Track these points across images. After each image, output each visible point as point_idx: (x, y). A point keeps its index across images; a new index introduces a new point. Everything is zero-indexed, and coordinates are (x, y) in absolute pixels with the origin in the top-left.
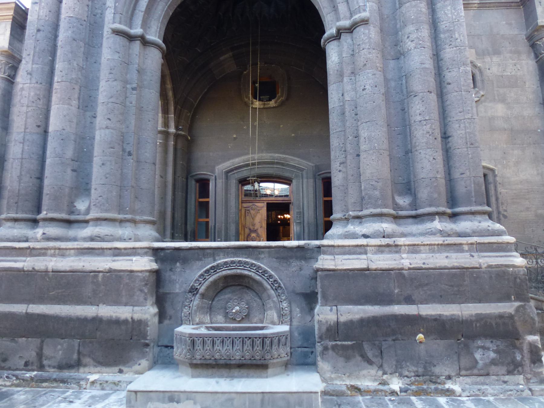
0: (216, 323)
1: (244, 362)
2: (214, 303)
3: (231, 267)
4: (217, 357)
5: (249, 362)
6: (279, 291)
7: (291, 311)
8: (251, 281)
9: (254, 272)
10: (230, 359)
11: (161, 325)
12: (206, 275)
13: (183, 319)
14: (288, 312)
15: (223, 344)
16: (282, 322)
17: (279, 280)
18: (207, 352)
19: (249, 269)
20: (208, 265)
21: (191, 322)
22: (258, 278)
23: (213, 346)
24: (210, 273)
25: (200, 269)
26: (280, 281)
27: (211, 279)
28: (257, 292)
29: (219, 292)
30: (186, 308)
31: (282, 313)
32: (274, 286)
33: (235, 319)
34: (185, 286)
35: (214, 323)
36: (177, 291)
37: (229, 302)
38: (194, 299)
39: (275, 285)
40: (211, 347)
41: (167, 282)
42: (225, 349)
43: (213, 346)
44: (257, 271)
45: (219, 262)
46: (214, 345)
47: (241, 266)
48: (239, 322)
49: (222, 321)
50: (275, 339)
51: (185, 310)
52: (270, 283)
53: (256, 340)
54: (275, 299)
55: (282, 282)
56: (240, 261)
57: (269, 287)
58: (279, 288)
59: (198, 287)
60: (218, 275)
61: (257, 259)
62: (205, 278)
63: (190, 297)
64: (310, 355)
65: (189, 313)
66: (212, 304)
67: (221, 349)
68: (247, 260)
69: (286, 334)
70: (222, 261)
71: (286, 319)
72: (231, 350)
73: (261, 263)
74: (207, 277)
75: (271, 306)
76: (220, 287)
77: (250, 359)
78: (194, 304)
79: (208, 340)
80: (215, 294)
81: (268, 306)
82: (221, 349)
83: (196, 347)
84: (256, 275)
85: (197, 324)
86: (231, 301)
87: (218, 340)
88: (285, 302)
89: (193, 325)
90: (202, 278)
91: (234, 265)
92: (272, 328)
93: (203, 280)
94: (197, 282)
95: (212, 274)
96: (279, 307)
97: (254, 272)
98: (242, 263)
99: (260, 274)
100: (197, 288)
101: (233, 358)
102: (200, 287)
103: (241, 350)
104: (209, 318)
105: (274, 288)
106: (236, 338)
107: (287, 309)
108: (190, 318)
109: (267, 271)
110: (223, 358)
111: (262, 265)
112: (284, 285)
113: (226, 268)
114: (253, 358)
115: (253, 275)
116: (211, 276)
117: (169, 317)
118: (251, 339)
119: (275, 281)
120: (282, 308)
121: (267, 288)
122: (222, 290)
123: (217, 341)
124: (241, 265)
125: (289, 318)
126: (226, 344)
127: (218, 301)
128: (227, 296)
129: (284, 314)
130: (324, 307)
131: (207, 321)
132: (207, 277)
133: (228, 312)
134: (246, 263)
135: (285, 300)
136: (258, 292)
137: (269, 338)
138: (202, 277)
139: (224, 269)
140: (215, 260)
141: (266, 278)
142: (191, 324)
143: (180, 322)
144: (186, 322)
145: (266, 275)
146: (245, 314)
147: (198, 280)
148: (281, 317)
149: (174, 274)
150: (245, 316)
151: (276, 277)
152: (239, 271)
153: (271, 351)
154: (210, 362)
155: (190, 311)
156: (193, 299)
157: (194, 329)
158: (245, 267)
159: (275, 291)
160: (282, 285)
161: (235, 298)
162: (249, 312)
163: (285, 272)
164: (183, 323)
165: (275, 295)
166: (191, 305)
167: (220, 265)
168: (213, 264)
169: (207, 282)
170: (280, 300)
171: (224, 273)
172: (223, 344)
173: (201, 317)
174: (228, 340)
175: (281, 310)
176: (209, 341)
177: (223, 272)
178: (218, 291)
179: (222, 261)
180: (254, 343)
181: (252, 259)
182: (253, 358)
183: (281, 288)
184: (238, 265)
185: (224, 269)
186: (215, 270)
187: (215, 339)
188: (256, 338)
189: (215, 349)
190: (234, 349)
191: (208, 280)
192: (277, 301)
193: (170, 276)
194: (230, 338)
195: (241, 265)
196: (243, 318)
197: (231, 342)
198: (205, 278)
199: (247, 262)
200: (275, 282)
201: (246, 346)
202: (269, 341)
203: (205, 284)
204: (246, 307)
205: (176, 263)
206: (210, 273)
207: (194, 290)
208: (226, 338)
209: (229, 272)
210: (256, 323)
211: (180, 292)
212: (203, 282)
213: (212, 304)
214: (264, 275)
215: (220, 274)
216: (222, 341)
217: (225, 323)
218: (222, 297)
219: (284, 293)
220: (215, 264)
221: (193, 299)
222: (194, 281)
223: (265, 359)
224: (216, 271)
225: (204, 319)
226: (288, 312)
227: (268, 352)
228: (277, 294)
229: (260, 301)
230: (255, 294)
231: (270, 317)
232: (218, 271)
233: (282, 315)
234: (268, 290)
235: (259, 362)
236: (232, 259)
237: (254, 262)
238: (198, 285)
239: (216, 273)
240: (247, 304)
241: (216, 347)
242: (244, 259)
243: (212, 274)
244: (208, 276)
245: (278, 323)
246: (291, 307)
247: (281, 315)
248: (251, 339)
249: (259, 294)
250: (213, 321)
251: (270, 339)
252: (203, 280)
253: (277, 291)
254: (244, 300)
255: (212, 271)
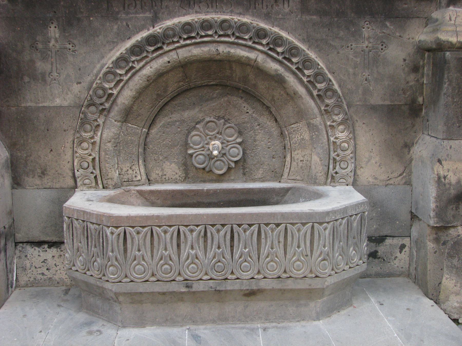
0: (162, 182)
1: (263, 284)
2: (154, 131)
3: (202, 37)
4: (188, 274)
5: (276, 285)
6: (327, 101)
7: (355, 152)
8: (251, 77)
9: (262, 52)
10: (226, 279)
11: (18, 192)
12: (133, 58)
13: (77, 174)
14: (349, 152)
15: (205, 241)
16: (333, 177)
17: (327, 72)
18: (162, 262)
19: (250, 43)
20: (138, 33)
21: (100, 182)
22: (273, 66)
23: (179, 246)
24: (145, 54)
25: (114, 44)
26: (330, 76)
27: (148, 71)
28: (266, 102)
29: (166, 104)
30: (85, 145)
31: (333, 155)
32: (315, 87)
33: (211, 171)
34: (76, 88)
35: (157, 182)
36: (58, 102)
37: (194, 128)
38: (104, 123)
39: (319, 86)
40: (172, 251)
41: (26, 79)
42: (210, 255)
43: (179, 246)
44: (270, 49)
45: (169, 23)
46: (182, 246)
47: (228, 36)
48: (220, 178)
49: (177, 176)
50: (341, 224)
51: (80, 151)
52: (305, 80)
53: (295, 228)
54: (318, 120)
55: (335, 78)
56: (224, 21)
57: (301, 90)
58: (329, 93)
59: (115, 92)
60: (166, 59)
61: (267, 17)
62: (132, 68)
63: (95, 116)
64: (398, 254)
65: (94, 159)
66: (148, 134)
67: (201, 254)
68: (246, 19)
69: (361, 209)
70: (176, 20)
71: (344, 171)
72: (228, 256)
73: (282, 28)
74: (137, 66)
75: (303, 139)
76: (170, 89)
77: (279, 277)
78: (104, 136)
79: (165, 232)
80: (156, 109)
81: (296, 138)
82: (201, 254)
83: (133, 252)
84: (269, 60)
85: (115, 187)
86: (197, 126)
87: (192, 231)
88: (341, 127)
89: (104, 188)
90: (121, 68)
91: (210, 33)
92: (318, 196)
93: (127, 72)
94: (111, 77)
95: (150, 56)
96: (325, 140)
97: (262, 52)
98: (230, 27)
99: (280, 58)
100: (111, 95)
101: (234, 277)
102: (119, 93)
103: (255, 257)
104: (142, 170)
105: (315, 93)
106: (239, 225)
107: (346, 145)
108: (97, 172)
109: (296, 48)
110: (205, 277)
111: (284, 34)
112: (340, 86)
113: (188, 42)
114: (284, 275)
115: (261, 58)
116: (147, 63)
117: (39, 171)
118: (282, 227)
119: (316, 75)
120: (334, 143)
121: (295, 93)
122: (173, 99)
123: (188, 233)
124: (229, 32)
125: (351, 167)
126: (216, 242)
127: (164, 126)
128: (187, 114)
129: (338, 158)
130: (451, 143)
131: (139, 178)
132: (137, 66)
133: (191, 155)
134: (244, 28)
135: (340, 124)
136: (269, 105)
137: (328, 223)
138: (123, 64)
139: (182, 42)
140: (155, 20)
141: (293, 68)
142: (101, 186)
143: (71, 182)
144: (87, 181)
145: (294, 60)
146: (235, 159)
147: (115, 74)
148: (331, 167)
149: (44, 58)
150: (236, 162)
151: (322, 65)
152: (222, 49)
153: (331, 255)
154: (174, 287)
155: (94, 155)
156: (101, 121)
157: (111, 200)
158: (238, 38)
159: (318, 101)
160: (336, 87)
161: (208, 119)
162: (244, 153)
163: (341, 52)
164: (79, 183)
165: (316, 111)
166: (97, 139)
167: (171, 32)
168: (151, 31)
169: (137, 78)
170: (328, 123)
171: (183, 54)
172: (205, 241)
173: (125, 169)
174: (218, 231)
175: (332, 148)
176: (168, 236)
177: (180, 51)
178: (166, 100)
179: (176, 20)
180: (289, 238)
181: (258, 16)
182: (284, 275)
183: (334, 92)
184: (222, 33)
185: (182, 42)
186: (159, 45)
187: (182, 229)
188: (293, 224)
189: (184, 256)
190: (236, 256)
191: (140, 74)
192: (322, 127)
193: (32, 61)
194: (223, 225)
195: (229, 32)
196: (229, 169)
197: (228, 237)
198: (132, 68)
199: (244, 24)
200: (319, 78)
201: (269, 243)
202: (327, 232)
203: (131, 84)
204: (239, 140)
205: (45, 26)
206: (145, 54)
207: (104, 100)
208: (213, 225)
209: (196, 51)
210: (262, 180)
211: (66, 104)
212: (125, 78)
213: (148, 134)
214: (289, 60)
215: (173, 56)
216: (202, 234)
217: (182, 182)
218: (175, 116)
219: (340, 106)
220: (158, 29)
221: (101, 121)
222: (101, 75)
223: (317, 276)
224: (161, 48)
225: (130, 171)
226: (349, 152)
227: (324, 260)
228: (323, 108)
229: (274, 124)
230: (259, 107)
231: (300, 164)
232: (166, 48)
233: (334, 159)
234: (300, 97)
235: (301, 285)
236: (203, 17)
237: (262, 25)
238: (112, 85)
239: (161, 55)
240: (240, 133)
241: (186, 251)
242: (236, 18)
243: (150, 56)
244: (139, 61)
245: (323, 179)
246: (355, 139)
247: (331, 161)
248: (282, 227)
249: (273, 110)
250: (153, 176)
251: (330, 226)
252: (127, 72)
253: (323, 101)
254: (233, 125)
255: (152, 48)
